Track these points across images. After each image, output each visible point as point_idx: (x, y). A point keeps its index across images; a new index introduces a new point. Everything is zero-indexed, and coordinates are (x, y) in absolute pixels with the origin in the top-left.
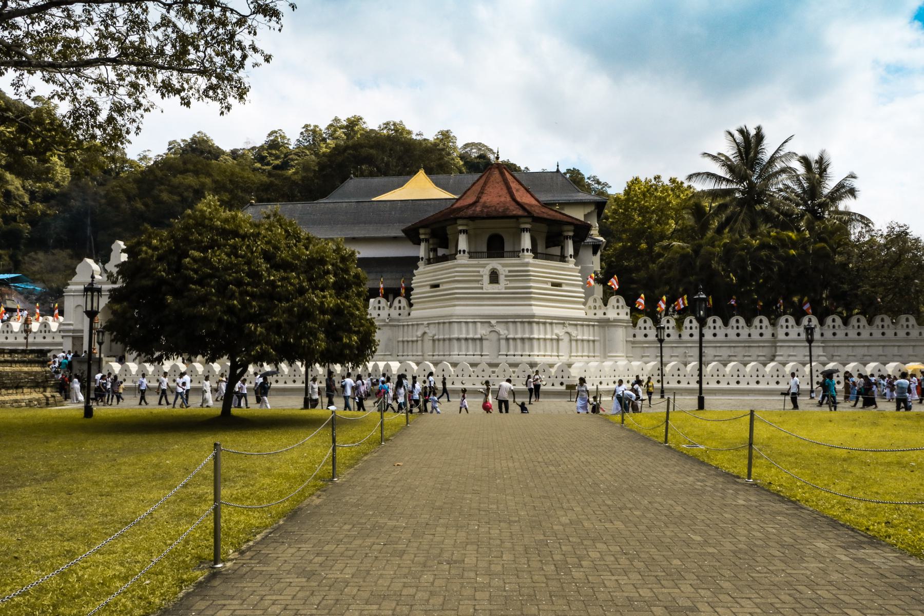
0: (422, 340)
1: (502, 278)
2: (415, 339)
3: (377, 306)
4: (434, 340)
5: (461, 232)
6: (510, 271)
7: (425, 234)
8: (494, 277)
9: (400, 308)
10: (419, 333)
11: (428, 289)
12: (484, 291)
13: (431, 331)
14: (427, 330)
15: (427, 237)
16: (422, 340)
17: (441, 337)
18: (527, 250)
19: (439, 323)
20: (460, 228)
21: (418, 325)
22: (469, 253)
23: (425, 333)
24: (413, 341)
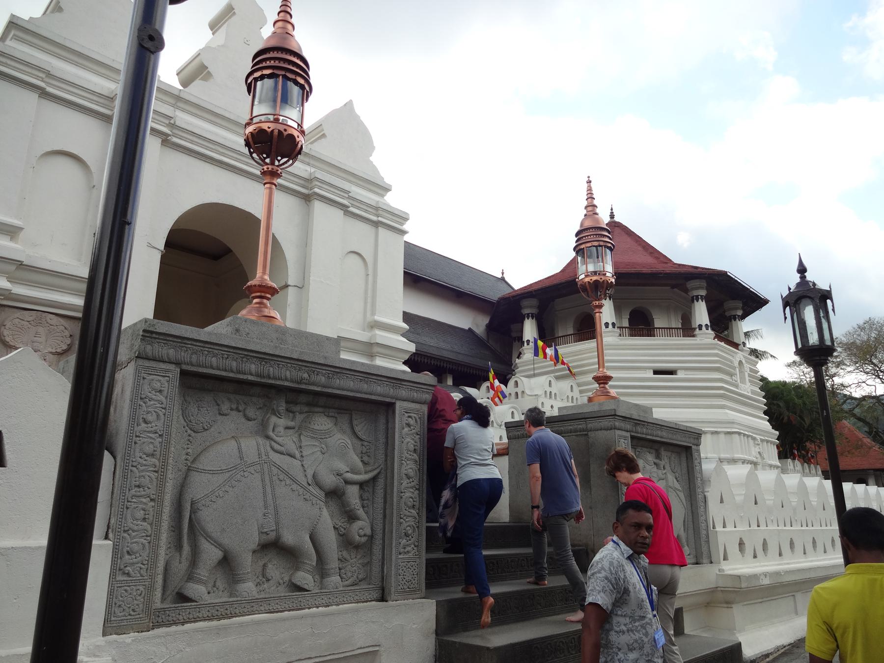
7: (531, 307)
15: (534, 311)
18: (700, 327)
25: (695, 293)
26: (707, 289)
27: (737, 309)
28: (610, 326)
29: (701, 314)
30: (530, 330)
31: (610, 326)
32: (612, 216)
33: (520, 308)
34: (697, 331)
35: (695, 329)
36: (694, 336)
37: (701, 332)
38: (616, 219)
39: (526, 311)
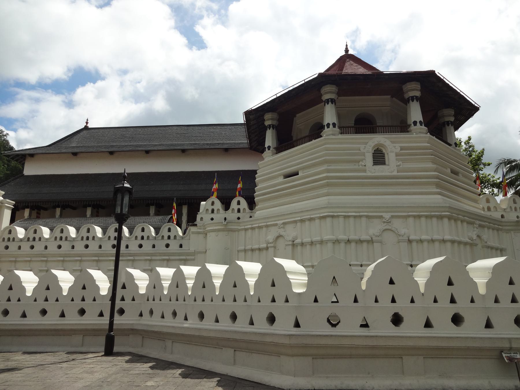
0: (275, 247)
1: (391, 157)
2: (264, 246)
3: (210, 208)
4: (294, 245)
5: (327, 101)
6: (402, 149)
8: (379, 157)
9: (239, 211)
10: (271, 238)
11: (281, 179)
12: (369, 174)
13: (290, 233)
14: (282, 232)
15: (275, 123)
16: (275, 247)
17: (307, 240)
18: (415, 123)
19: (302, 221)
20: (325, 97)
21: (267, 226)
22: (340, 128)
23: (279, 236)
24: (260, 249)
25: (412, 94)
26: (421, 91)
27: (450, 116)
28: (331, 126)
29: (415, 113)
30: (270, 139)
31: (331, 126)
32: (347, 51)
33: (264, 120)
34: (413, 127)
35: (410, 125)
36: (408, 132)
37: (415, 127)
38: (351, 52)
39: (267, 123)
